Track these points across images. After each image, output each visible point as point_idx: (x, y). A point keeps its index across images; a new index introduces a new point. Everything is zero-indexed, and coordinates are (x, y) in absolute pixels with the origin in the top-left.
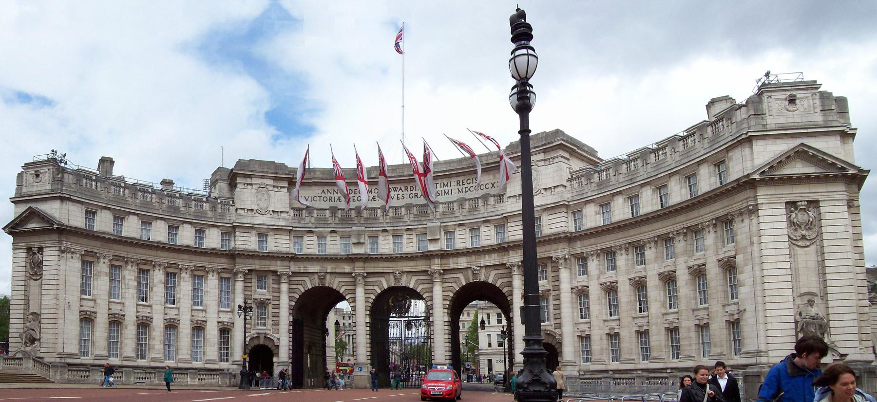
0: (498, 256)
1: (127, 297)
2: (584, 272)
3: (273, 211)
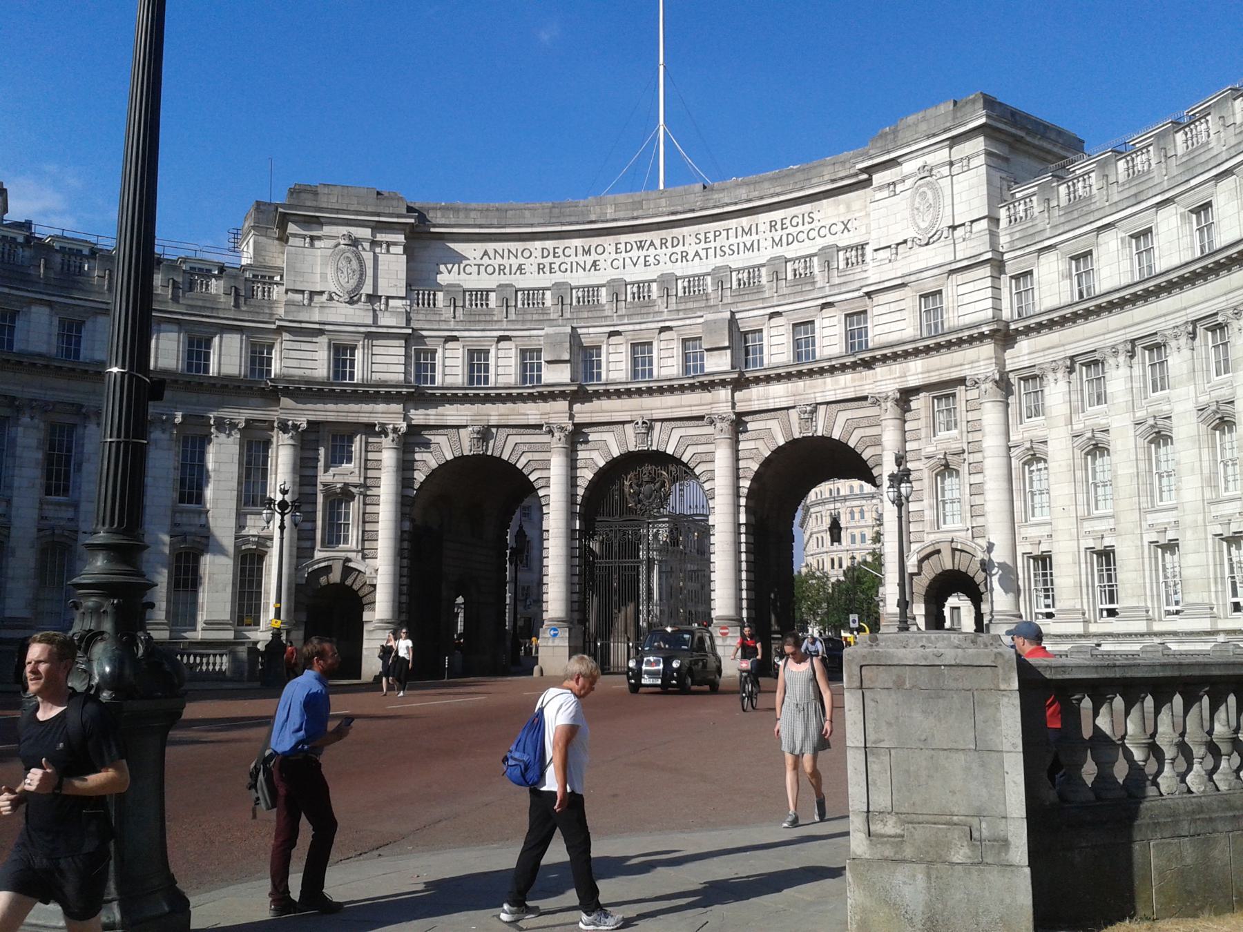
0: (853, 380)
1: (16, 484)
2: (1036, 411)
3: (368, 296)
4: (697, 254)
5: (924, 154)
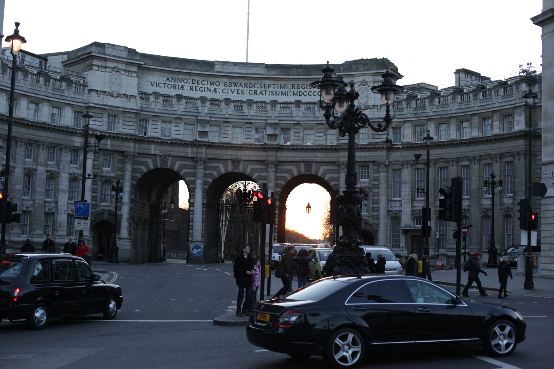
3: (123, 94)
4: (261, 92)
5: (364, 76)
